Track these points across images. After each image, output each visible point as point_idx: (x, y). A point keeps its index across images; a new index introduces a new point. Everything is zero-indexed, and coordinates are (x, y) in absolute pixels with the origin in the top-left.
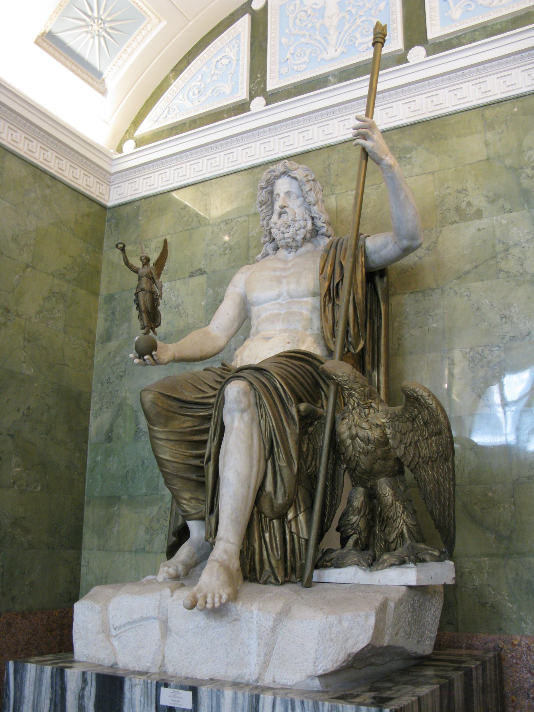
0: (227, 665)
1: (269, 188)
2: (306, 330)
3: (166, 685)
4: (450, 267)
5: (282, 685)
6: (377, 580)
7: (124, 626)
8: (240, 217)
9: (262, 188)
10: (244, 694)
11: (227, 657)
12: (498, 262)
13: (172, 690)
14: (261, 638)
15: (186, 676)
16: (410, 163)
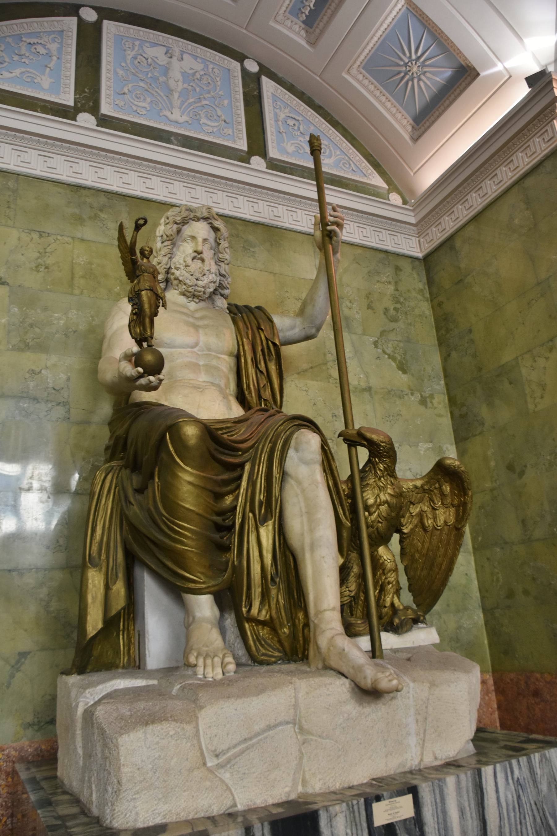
0: (386, 756)
1: (180, 226)
3: (378, 798)
5: (445, 759)
7: (235, 746)
8: (61, 236)
11: (385, 746)
12: (328, 369)
13: (387, 802)
14: (419, 714)
15: (341, 786)
16: (254, 257)
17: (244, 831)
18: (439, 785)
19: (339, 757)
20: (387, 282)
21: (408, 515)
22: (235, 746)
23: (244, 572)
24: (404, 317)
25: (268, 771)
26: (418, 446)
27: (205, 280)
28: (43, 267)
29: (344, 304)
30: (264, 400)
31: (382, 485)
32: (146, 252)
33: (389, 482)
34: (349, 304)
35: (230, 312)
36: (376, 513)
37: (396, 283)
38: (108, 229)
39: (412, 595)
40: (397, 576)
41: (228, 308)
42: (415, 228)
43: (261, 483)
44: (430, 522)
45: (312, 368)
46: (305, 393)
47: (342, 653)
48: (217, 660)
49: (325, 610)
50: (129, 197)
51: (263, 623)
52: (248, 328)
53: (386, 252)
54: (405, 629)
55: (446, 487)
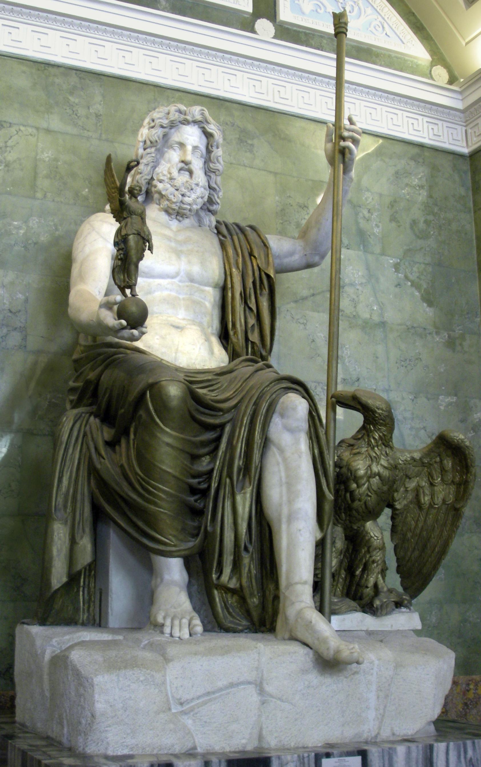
0: (343, 725)
2: (208, 327)
3: (328, 755)
4: (288, 287)
5: (402, 736)
6: (390, 626)
7: (199, 698)
9: (162, 127)
10: (417, 747)
11: (343, 716)
13: (336, 759)
14: (381, 690)
15: (296, 746)
16: (251, 151)
17: (203, 764)
18: (389, 752)
19: (296, 720)
20: (418, 185)
21: (402, 489)
22: (199, 698)
23: (217, 538)
24: (436, 233)
25: (228, 722)
26: (438, 399)
27: (194, 196)
28: (4, 165)
29: (361, 215)
30: (252, 342)
31: (374, 455)
32: (136, 192)
33: (384, 453)
34: (367, 215)
35: (219, 233)
36: (366, 486)
37: (431, 187)
38: (78, 117)
39: (400, 577)
40: (384, 556)
41: (216, 228)
42: (462, 115)
43: (240, 448)
44: (426, 498)
45: (313, 295)
46: (302, 326)
47: (309, 625)
48: (185, 621)
49: (297, 583)
50: (104, 75)
51: (233, 591)
52: (238, 255)
53: (421, 146)
54: (384, 612)
55: (448, 462)
